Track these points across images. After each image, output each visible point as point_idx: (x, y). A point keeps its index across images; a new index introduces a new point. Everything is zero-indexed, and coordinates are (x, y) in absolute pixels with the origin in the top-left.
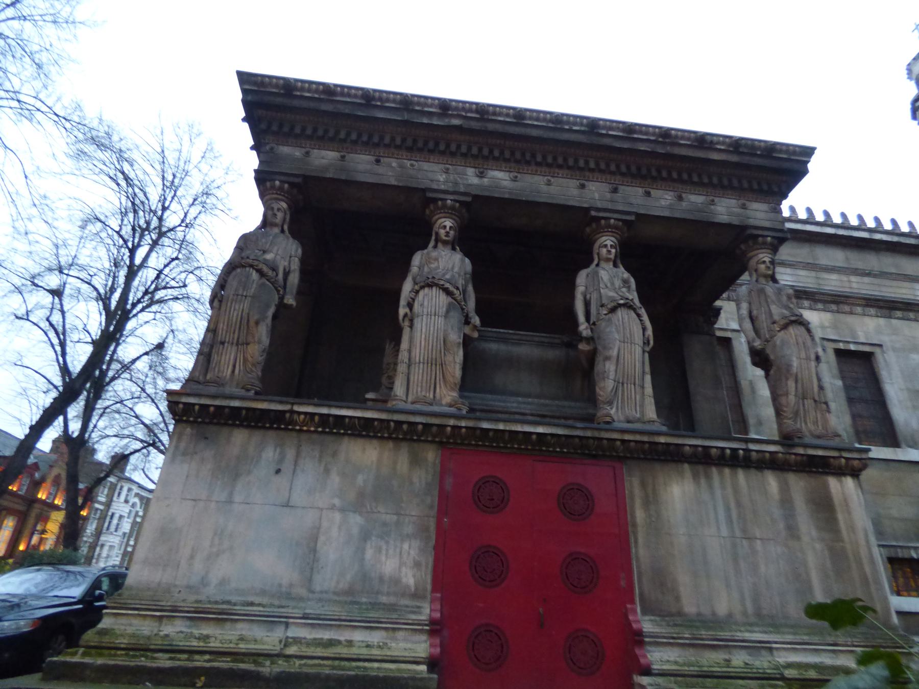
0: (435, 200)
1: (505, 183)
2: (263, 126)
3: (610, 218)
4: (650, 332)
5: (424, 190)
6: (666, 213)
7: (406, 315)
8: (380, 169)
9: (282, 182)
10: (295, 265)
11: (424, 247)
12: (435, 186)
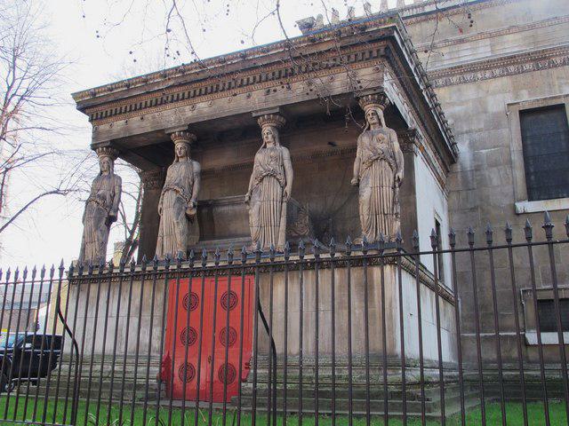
1: (205, 110)
3: (264, 115)
4: (288, 189)
6: (300, 100)
8: (144, 124)
9: (102, 148)
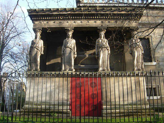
0: (67, 29)
2: (33, 19)
5: (64, 27)
7: (63, 53)
10: (43, 45)
11: (66, 39)
12: (66, 26)
